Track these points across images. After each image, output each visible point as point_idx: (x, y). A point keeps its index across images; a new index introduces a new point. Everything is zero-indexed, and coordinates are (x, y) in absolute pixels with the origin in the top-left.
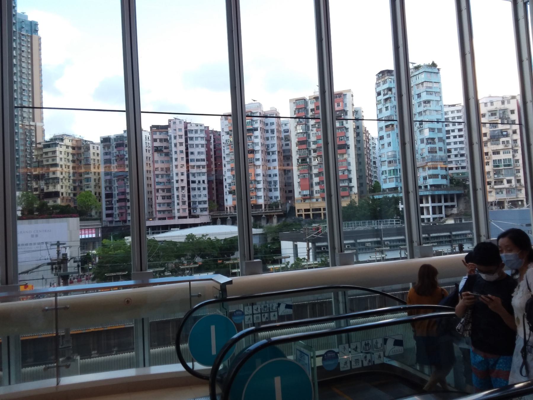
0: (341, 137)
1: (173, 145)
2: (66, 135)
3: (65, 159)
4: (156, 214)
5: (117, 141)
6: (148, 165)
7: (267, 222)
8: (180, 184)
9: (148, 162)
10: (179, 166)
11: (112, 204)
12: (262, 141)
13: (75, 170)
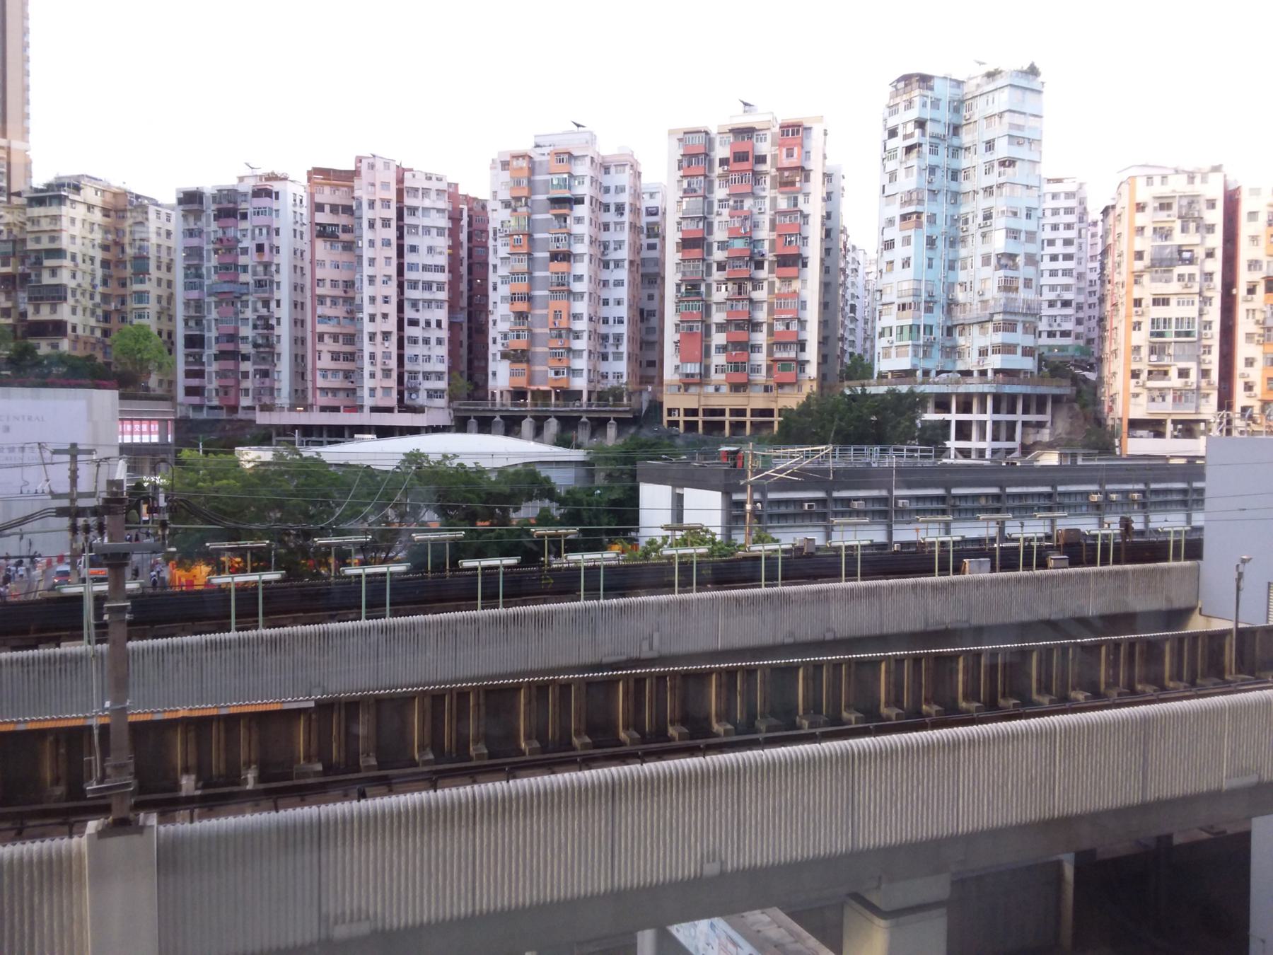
0: (791, 235)
1: (365, 224)
2: (87, 177)
3: (84, 238)
4: (314, 395)
5: (220, 203)
6: (299, 270)
7: (592, 435)
8: (380, 326)
9: (299, 264)
10: (379, 280)
11: (203, 364)
12: (594, 231)
13: (109, 268)
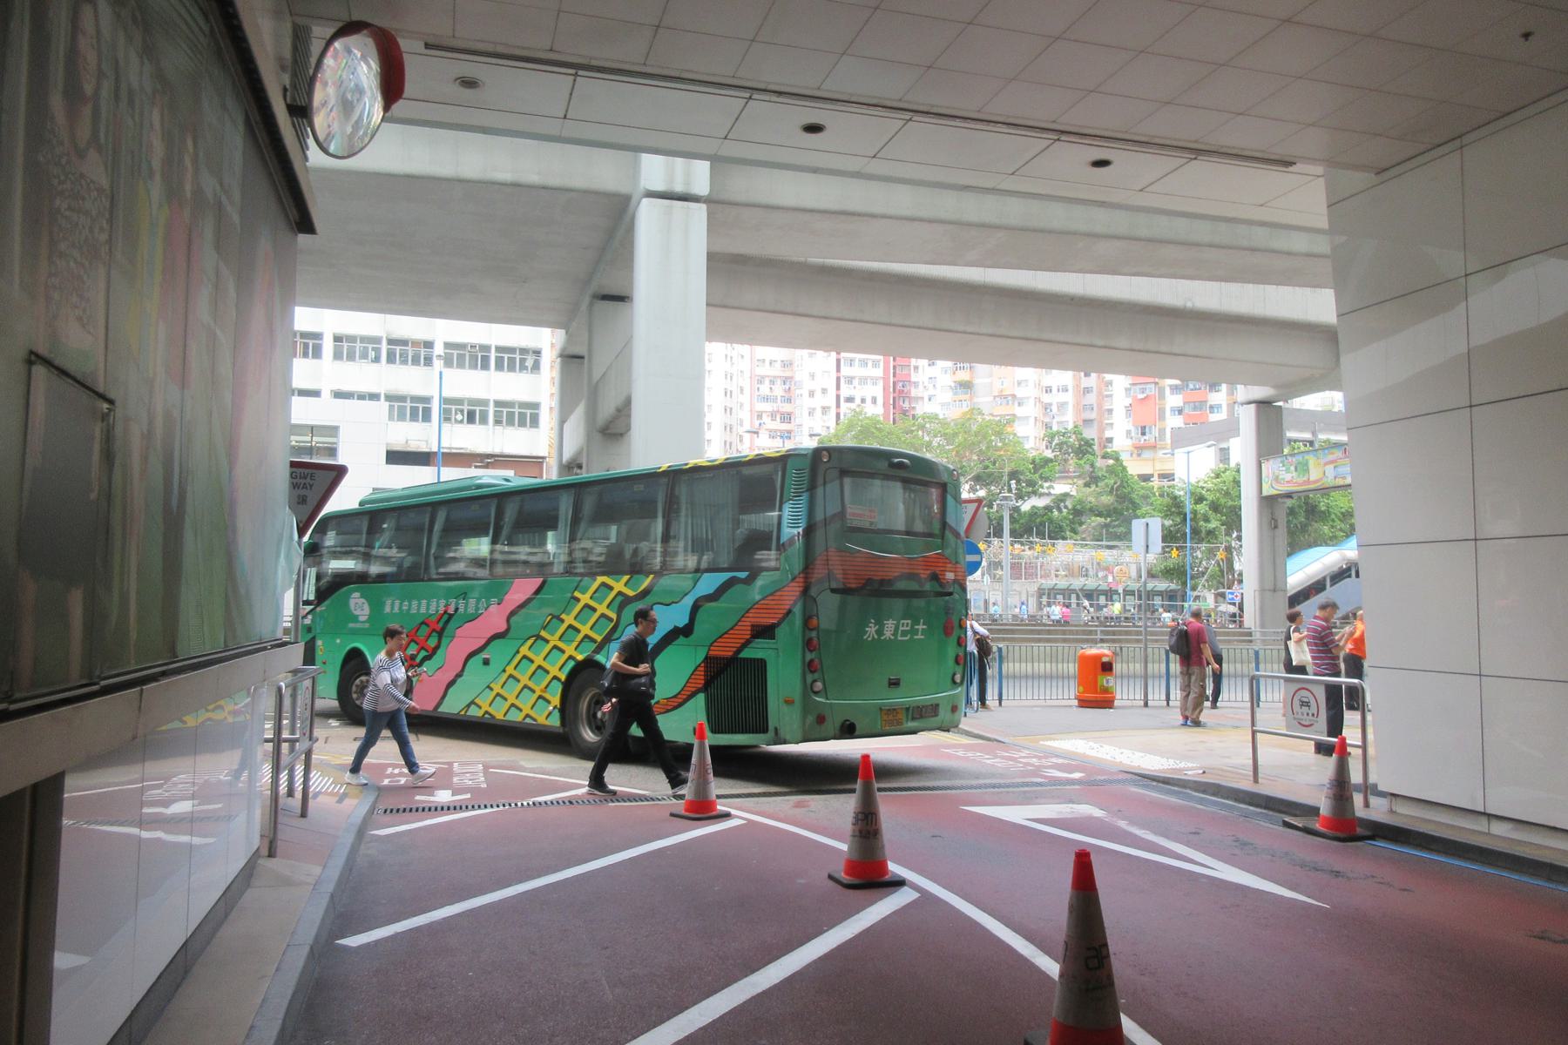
6: (729, 358)
8: (819, 401)
